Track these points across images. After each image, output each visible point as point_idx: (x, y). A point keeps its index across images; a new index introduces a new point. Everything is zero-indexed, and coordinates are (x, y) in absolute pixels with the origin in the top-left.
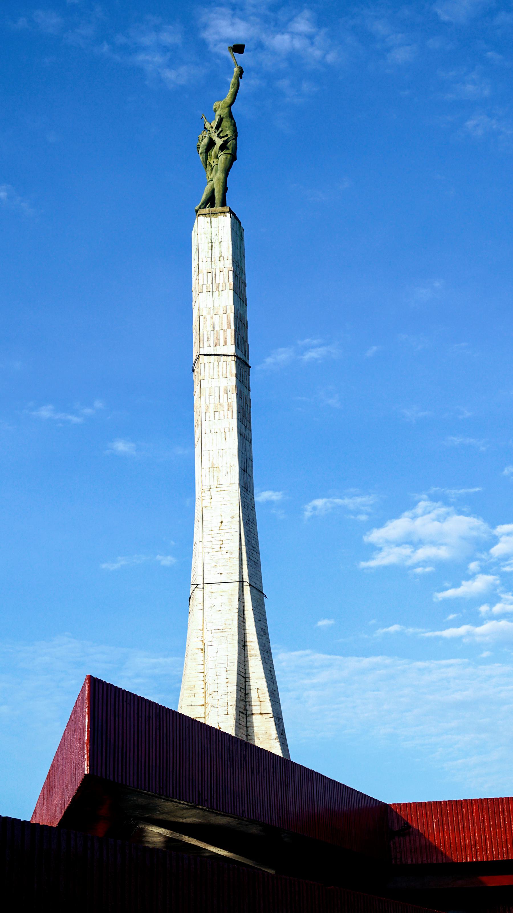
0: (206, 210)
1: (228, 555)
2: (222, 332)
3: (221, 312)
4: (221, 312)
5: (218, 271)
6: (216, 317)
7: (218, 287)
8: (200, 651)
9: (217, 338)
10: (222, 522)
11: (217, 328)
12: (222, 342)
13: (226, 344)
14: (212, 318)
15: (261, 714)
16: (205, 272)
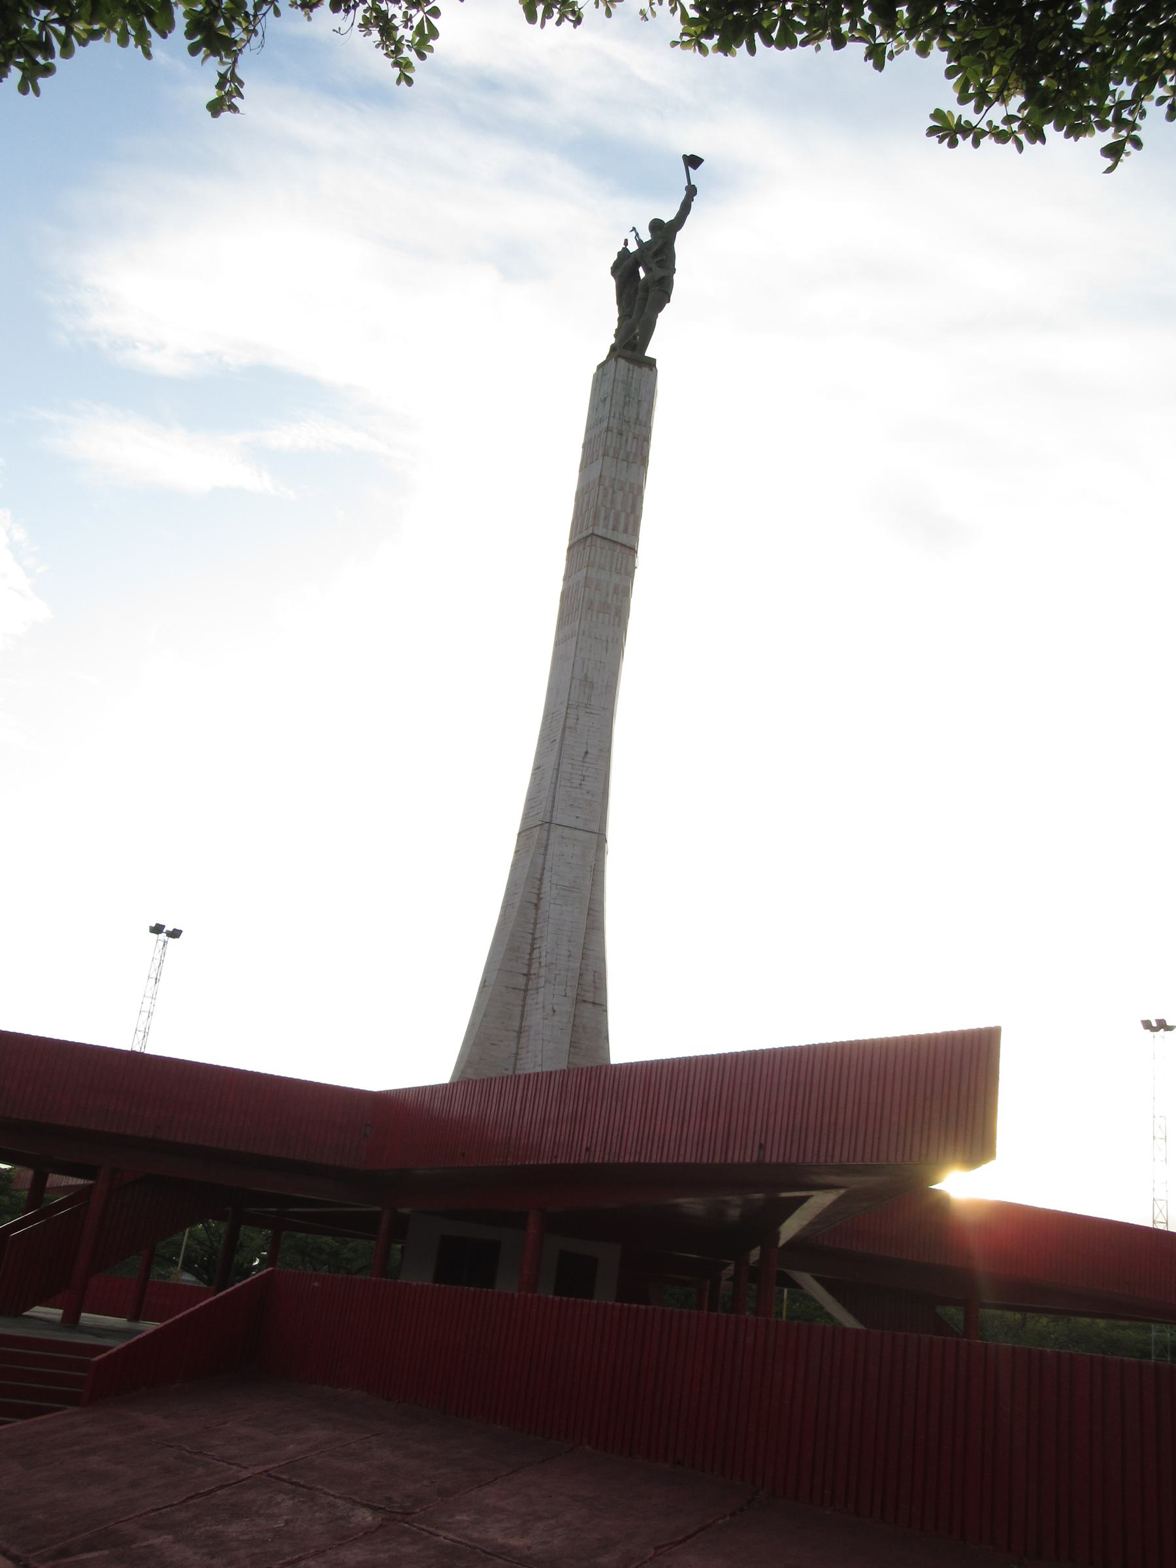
0: (629, 353)
1: (588, 797)
2: (623, 515)
3: (627, 488)
4: (627, 488)
5: (631, 436)
6: (620, 495)
7: (628, 456)
8: (533, 906)
9: (617, 520)
10: (587, 753)
11: (619, 507)
12: (621, 527)
13: (626, 531)
14: (614, 492)
15: (594, 1003)
16: (615, 431)
